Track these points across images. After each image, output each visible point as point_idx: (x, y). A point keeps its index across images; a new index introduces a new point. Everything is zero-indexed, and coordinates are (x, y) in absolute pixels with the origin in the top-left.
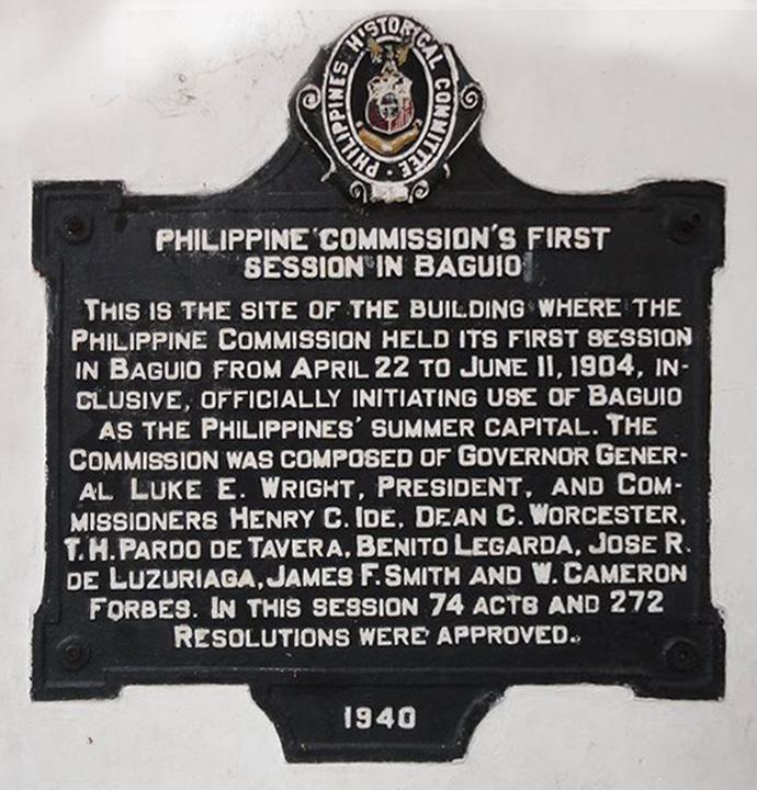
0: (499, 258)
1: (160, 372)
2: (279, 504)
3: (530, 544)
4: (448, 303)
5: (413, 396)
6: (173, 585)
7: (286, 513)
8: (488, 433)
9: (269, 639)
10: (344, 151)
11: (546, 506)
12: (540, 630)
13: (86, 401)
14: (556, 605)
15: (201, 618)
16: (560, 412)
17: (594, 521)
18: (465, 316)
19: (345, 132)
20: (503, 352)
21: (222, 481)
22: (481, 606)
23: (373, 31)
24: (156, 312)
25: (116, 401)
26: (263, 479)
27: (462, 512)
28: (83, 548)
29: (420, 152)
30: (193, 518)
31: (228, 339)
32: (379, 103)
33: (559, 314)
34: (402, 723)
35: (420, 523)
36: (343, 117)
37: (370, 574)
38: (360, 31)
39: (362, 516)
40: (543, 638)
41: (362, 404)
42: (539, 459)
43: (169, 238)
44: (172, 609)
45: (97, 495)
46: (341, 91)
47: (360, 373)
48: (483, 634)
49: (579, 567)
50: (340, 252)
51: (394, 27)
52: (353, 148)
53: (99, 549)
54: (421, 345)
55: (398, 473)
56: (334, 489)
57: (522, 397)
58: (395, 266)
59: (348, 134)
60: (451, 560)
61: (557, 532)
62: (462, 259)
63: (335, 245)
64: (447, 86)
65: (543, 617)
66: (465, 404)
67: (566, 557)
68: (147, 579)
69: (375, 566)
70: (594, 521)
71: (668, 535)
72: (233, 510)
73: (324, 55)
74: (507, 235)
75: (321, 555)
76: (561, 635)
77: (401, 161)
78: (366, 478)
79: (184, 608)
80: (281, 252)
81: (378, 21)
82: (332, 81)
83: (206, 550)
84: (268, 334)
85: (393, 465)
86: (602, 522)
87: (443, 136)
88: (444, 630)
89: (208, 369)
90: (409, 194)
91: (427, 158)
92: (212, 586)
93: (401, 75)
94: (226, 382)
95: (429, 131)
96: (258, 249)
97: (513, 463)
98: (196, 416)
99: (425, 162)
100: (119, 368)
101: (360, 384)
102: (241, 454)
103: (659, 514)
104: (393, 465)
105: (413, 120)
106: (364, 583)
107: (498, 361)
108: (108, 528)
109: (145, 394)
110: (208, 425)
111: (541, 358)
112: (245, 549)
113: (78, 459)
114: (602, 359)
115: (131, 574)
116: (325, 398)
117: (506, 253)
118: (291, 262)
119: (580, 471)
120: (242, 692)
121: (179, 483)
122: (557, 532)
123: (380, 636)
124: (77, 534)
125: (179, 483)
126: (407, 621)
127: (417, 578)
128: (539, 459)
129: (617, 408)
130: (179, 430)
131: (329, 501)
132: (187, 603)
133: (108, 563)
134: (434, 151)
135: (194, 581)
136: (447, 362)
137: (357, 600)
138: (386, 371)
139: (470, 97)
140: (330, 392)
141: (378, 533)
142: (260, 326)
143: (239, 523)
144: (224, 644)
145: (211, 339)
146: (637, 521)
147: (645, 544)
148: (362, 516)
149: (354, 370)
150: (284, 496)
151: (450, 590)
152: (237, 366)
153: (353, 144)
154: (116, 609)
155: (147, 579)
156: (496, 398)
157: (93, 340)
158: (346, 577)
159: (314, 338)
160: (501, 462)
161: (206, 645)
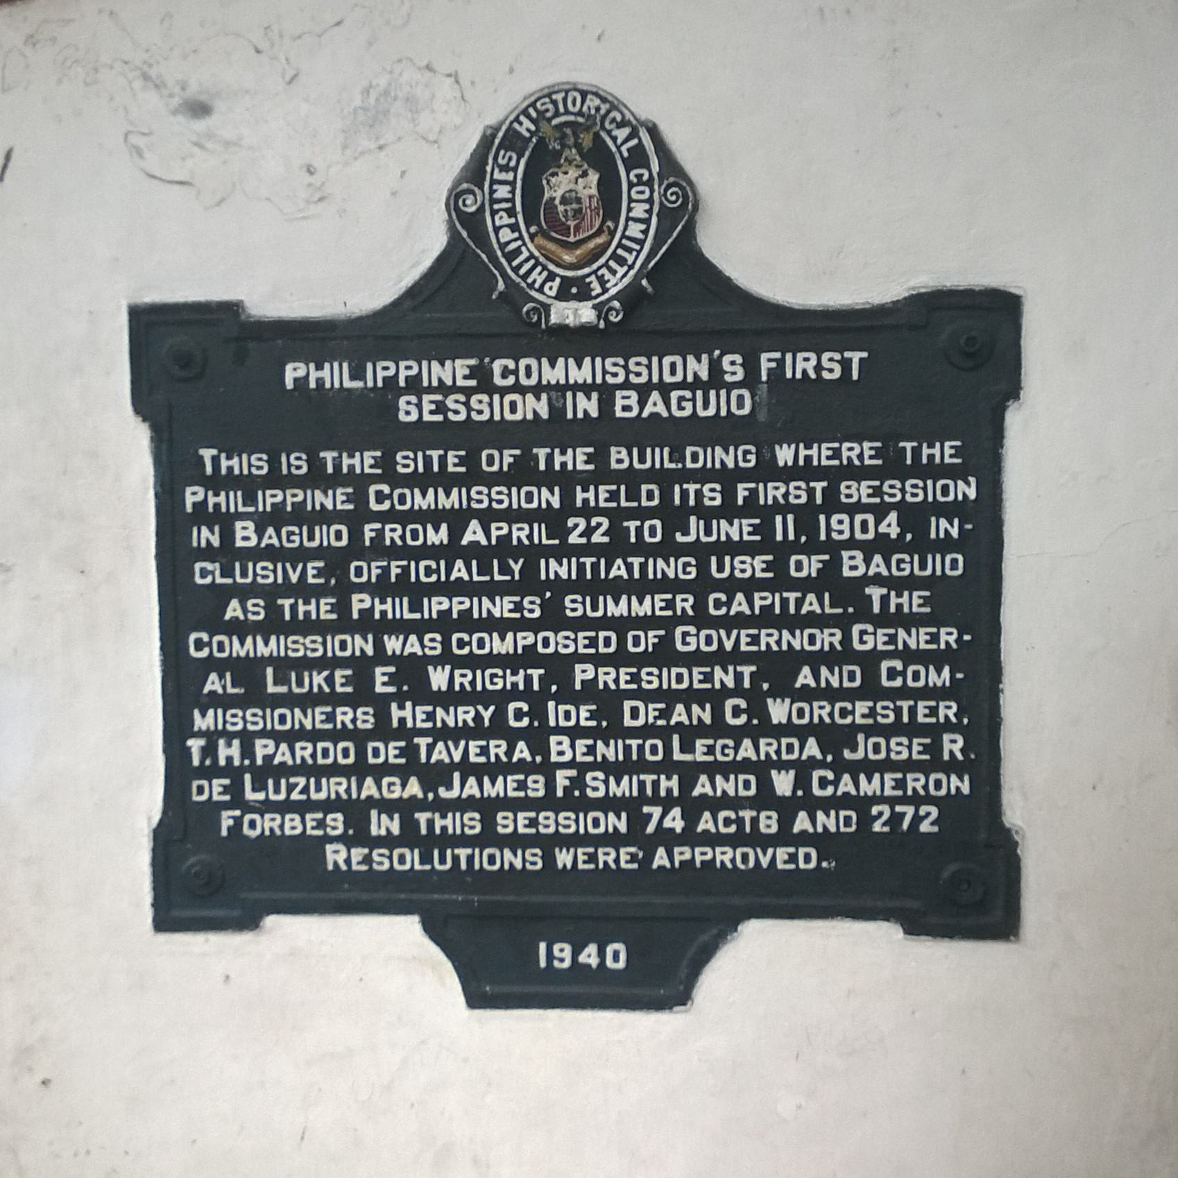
0: (723, 393)
1: (297, 538)
2: (451, 698)
3: (768, 747)
4: (657, 450)
5: (615, 566)
6: (322, 795)
7: (460, 709)
8: (712, 611)
9: (443, 860)
10: (515, 263)
11: (788, 701)
12: (782, 853)
13: (206, 574)
14: (802, 823)
15: (357, 835)
16: (805, 585)
17: (849, 720)
18: (680, 466)
19: (515, 240)
20: (729, 511)
21: (379, 671)
22: (706, 823)
23: (547, 110)
24: (289, 465)
25: (244, 574)
26: (430, 668)
27: (680, 708)
28: (209, 751)
29: (612, 263)
30: (344, 716)
31: (380, 497)
32: (557, 202)
33: (801, 462)
34: (609, 963)
35: (628, 722)
36: (513, 220)
37: (567, 783)
38: (531, 111)
39: (555, 713)
40: (785, 862)
41: (552, 576)
42: (779, 642)
43: (301, 373)
44: (321, 824)
45: (224, 687)
46: (508, 188)
47: (548, 538)
48: (709, 857)
49: (830, 776)
50: (517, 388)
51: (574, 104)
52: (527, 260)
53: (229, 752)
54: (624, 504)
55: (598, 661)
56: (520, 679)
57: (754, 566)
58: (588, 406)
59: (519, 243)
60: (667, 766)
61: (802, 733)
62: (674, 395)
63: (511, 380)
64: (646, 177)
65: (785, 836)
66: (682, 576)
67: (813, 763)
68: (291, 788)
69: (573, 773)
70: (849, 720)
71: (946, 737)
72: (394, 706)
73: (486, 142)
74: (733, 363)
75: (504, 759)
76: (808, 860)
77: (589, 275)
78: (560, 667)
79: (336, 823)
80: (443, 388)
81: (554, 97)
82: (497, 176)
83: (361, 753)
84: (431, 490)
85: (592, 651)
86: (859, 721)
87: (641, 243)
88: (661, 851)
89: (356, 535)
90: (599, 317)
91: (621, 271)
92: (370, 798)
93: (586, 166)
94: (379, 549)
95: (623, 236)
96: (414, 385)
97: (743, 648)
98: (344, 592)
99: (619, 275)
100: (246, 533)
101: (549, 552)
102: (401, 637)
103: (933, 712)
104: (592, 651)
105: (603, 222)
106: (560, 793)
107: (723, 523)
108: (240, 727)
109: (279, 566)
110: (360, 602)
111: (779, 519)
112: (410, 752)
113: (199, 645)
114: (858, 518)
115: (270, 782)
116: (505, 569)
117: (731, 387)
118: (457, 401)
119: (831, 658)
120: (410, 926)
121: (325, 673)
122: (802, 733)
123: (581, 858)
124: (200, 734)
125: (325, 673)
126: (613, 840)
127: (624, 788)
128: (779, 642)
129: (878, 580)
130: (324, 609)
131: (512, 694)
132: (340, 816)
133: (242, 770)
134: (630, 262)
135: (348, 790)
136: (658, 523)
137: (551, 814)
138: (580, 536)
139: (672, 194)
140: (511, 562)
141: (575, 733)
142: (422, 481)
143: (402, 721)
144: (386, 866)
145: (359, 498)
146: (906, 719)
147: (916, 748)
148: (555, 713)
149: (540, 534)
150: (457, 688)
151: (667, 803)
152: (393, 530)
153: (525, 254)
154: (252, 824)
155: (291, 788)
156: (720, 569)
157: (212, 500)
158: (537, 787)
159: (489, 495)
160: (729, 646)
161: (364, 868)
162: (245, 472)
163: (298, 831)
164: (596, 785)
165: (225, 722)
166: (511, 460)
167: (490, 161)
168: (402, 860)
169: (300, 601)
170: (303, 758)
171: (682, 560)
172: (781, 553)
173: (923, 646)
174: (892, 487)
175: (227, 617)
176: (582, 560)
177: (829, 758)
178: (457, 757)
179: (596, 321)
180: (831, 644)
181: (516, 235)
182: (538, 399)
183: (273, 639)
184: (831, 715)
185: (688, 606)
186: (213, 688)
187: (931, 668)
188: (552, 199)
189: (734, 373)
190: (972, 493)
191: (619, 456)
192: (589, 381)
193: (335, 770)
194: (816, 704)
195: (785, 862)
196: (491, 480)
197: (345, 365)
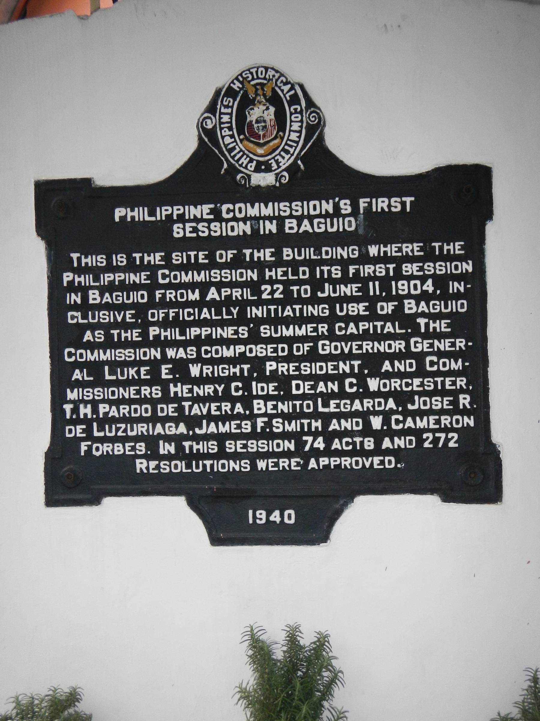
0: (341, 219)
1: (121, 298)
2: (201, 381)
3: (368, 403)
4: (307, 249)
6: (134, 433)
7: (206, 387)
8: (338, 333)
9: (197, 467)
10: (232, 154)
11: (378, 379)
12: (376, 460)
14: (387, 443)
16: (385, 318)
17: (410, 388)
18: (319, 257)
19: (232, 142)
20: (345, 280)
21: (163, 367)
22: (336, 445)
23: (248, 77)
24: (117, 261)
25: (93, 317)
26: (190, 365)
27: (321, 384)
28: (75, 410)
29: (282, 153)
30: (145, 391)
31: (164, 276)
32: (254, 123)
33: (382, 254)
34: (286, 521)
35: (294, 392)
36: (231, 133)
37: (263, 425)
39: (256, 387)
40: (378, 465)
41: (254, 316)
42: (372, 348)
43: (123, 213)
44: (133, 448)
45: (83, 377)
46: (228, 116)
48: (338, 463)
49: (401, 418)
50: (235, 219)
51: (262, 74)
52: (239, 153)
53: (85, 411)
54: (291, 277)
55: (278, 359)
56: (237, 370)
57: (360, 308)
58: (272, 227)
59: (235, 144)
60: (316, 415)
61: (386, 396)
62: (316, 221)
63: (231, 215)
64: (299, 110)
65: (378, 451)
66: (321, 314)
67: (392, 412)
68: (117, 429)
69: (266, 419)
70: (410, 388)
71: (461, 396)
72: (171, 385)
73: (218, 93)
74: (345, 204)
75: (230, 413)
76: (390, 463)
77: (270, 160)
79: (141, 447)
80: (196, 220)
81: (251, 70)
82: (223, 110)
83: (154, 410)
84: (190, 272)
85: (275, 355)
86: (415, 389)
87: (297, 143)
88: (313, 460)
89: (152, 296)
90: (276, 181)
91: (287, 157)
92: (159, 434)
93: (268, 104)
94: (164, 304)
95: (288, 139)
96: (181, 219)
97: (354, 351)
98: (145, 325)
100: (94, 296)
102: (175, 349)
103: (454, 383)
104: (275, 355)
105: (277, 133)
106: (259, 430)
108: (91, 398)
109: (112, 313)
110: (153, 331)
111: (371, 284)
112: (180, 409)
113: (70, 355)
114: (412, 283)
115: (107, 427)
116: (229, 313)
117: (345, 216)
118: (203, 226)
119: (400, 356)
120: (180, 502)
121: (136, 369)
122: (386, 396)
123: (270, 464)
124: (71, 402)
125: (136, 369)
126: (288, 454)
127: (293, 427)
128: (372, 348)
129: (423, 315)
130: (134, 335)
131: (234, 378)
132: (143, 444)
133: (92, 420)
134: (291, 153)
135: (148, 431)
136: (308, 287)
137: (254, 442)
138: (268, 294)
139: (312, 117)
140: (232, 309)
141: (267, 398)
142: (185, 268)
143: (176, 393)
144: (168, 470)
145: (153, 277)
146: (440, 388)
147: (445, 403)
148: (256, 387)
149: (247, 294)
150: (204, 375)
151: (315, 434)
152: (171, 293)
153: (238, 150)
154: (97, 449)
155: (117, 429)
156: (341, 310)
157: (77, 279)
158: (246, 426)
159: (220, 274)
160: (346, 350)
162: (94, 265)
163: (122, 452)
164: (278, 425)
165: (83, 395)
166: (232, 256)
167: (219, 103)
168: (176, 466)
169: (123, 331)
170: (124, 414)
171: (321, 306)
172: (373, 301)
173: (447, 349)
174: (429, 266)
175: (85, 340)
176: (269, 307)
177: (400, 409)
178: (205, 411)
179: (274, 183)
180: (400, 349)
181: (233, 140)
182: (245, 224)
183: (108, 351)
184: (401, 386)
185: (325, 330)
186: (77, 377)
187: (452, 360)
188: (251, 122)
189: (346, 209)
190: (470, 269)
191: (288, 253)
192: (272, 215)
193: (141, 420)
194: (392, 381)
195: (378, 465)
196: (221, 266)
197: (146, 209)
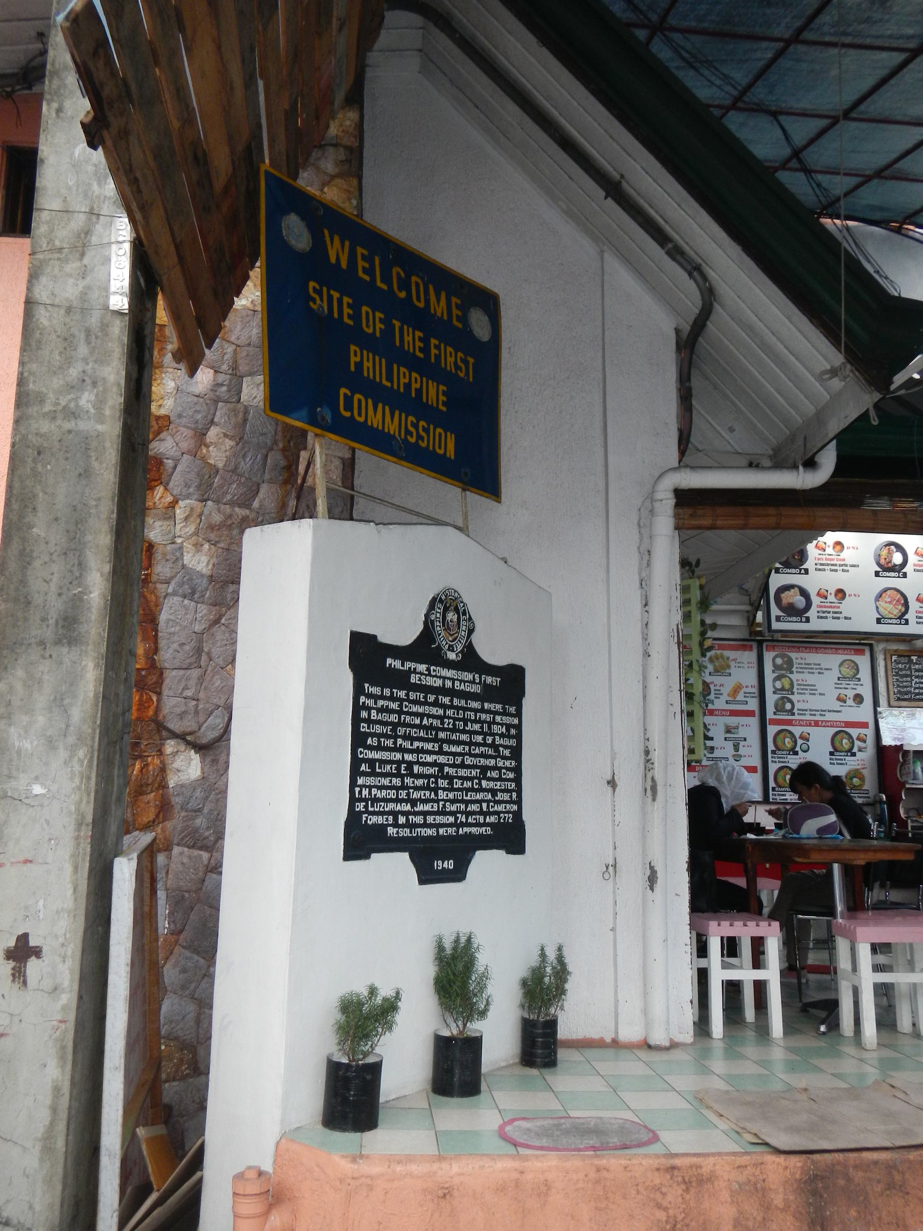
13: (364, 727)
15: (396, 825)
21: (403, 765)
28: (360, 792)
30: (394, 780)
57: (479, 738)
78: (441, 769)
110: (400, 741)
113: (361, 753)
126: (450, 825)
127: (454, 808)
130: (390, 743)
133: (369, 799)
